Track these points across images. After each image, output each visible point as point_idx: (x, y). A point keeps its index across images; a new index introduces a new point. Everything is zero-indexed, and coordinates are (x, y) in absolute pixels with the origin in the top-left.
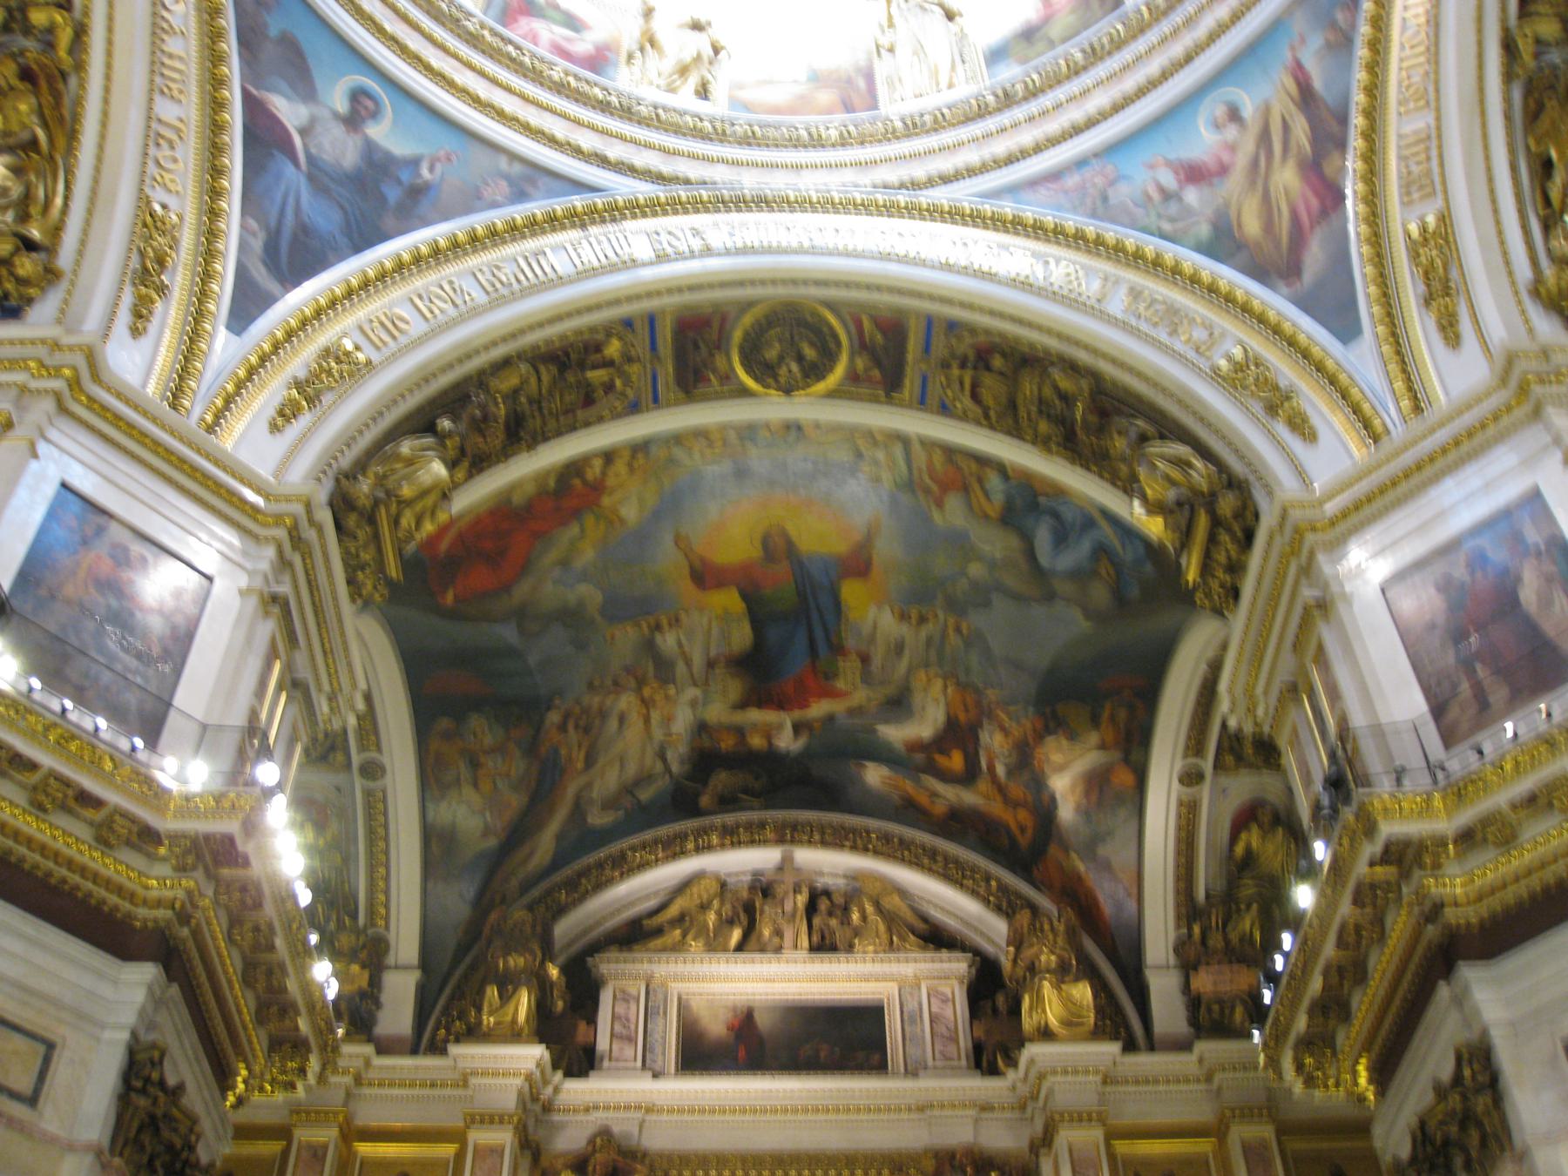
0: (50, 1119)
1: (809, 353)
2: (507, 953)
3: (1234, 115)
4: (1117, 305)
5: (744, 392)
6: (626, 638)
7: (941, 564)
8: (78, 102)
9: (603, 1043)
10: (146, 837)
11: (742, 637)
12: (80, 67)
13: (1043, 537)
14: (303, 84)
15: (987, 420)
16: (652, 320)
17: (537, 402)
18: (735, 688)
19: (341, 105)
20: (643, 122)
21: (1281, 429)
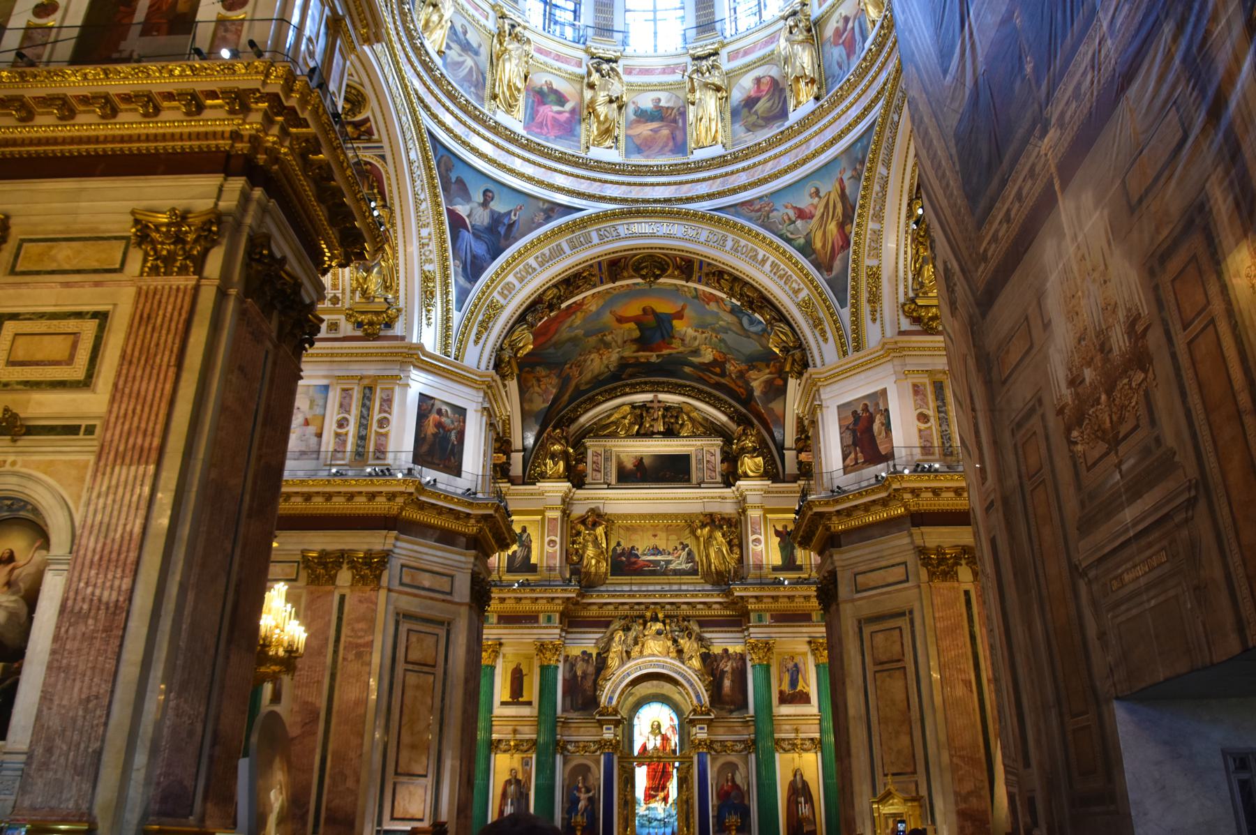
2: (553, 444)
3: (817, 193)
4: (767, 267)
6: (593, 340)
7: (709, 319)
10: (468, 515)
11: (636, 334)
12: (393, 225)
13: (745, 321)
14: (466, 196)
15: (721, 290)
16: (599, 263)
17: (559, 298)
18: (634, 347)
19: (481, 200)
20: (592, 169)
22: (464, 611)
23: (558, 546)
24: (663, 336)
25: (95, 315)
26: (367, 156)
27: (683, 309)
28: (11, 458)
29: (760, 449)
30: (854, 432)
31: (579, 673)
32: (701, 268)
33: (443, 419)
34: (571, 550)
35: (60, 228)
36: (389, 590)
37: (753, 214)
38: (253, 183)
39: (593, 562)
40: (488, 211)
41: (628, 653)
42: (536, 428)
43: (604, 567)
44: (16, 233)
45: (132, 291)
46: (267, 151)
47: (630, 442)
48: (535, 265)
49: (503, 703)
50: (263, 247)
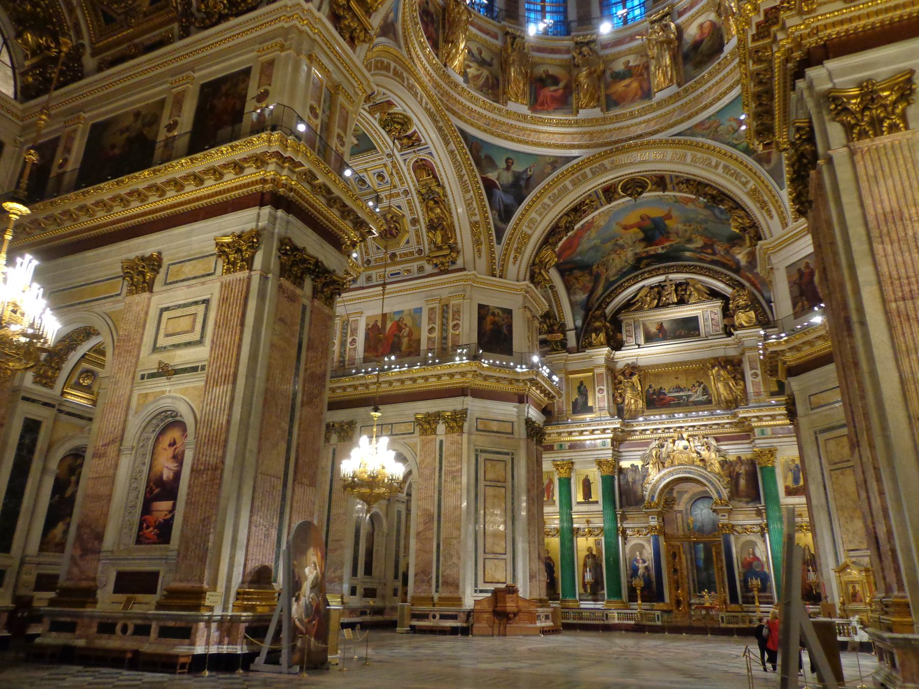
0: (516, 435)
1: (640, 190)
2: (595, 322)
5: (624, 197)
7: (692, 215)
8: (449, 205)
9: (624, 339)
10: (518, 381)
12: (446, 196)
13: (717, 211)
15: (692, 193)
16: (595, 192)
17: (570, 222)
18: (643, 245)
19: (504, 166)
21: (765, 214)
22: (523, 444)
23: (605, 393)
24: (661, 234)
25: (204, 301)
26: (422, 155)
27: (670, 211)
28: (168, 389)
29: (754, 304)
30: (800, 285)
31: (630, 480)
32: (672, 181)
33: (497, 319)
34: (616, 394)
35: (185, 254)
36: (470, 434)
37: (705, 132)
38: (277, 206)
39: (633, 401)
40: (510, 173)
41: (663, 463)
42: (582, 312)
43: (641, 404)
44: (166, 261)
45: (219, 284)
46: (284, 186)
47: (652, 313)
48: (549, 202)
49: (579, 503)
50: (286, 245)
